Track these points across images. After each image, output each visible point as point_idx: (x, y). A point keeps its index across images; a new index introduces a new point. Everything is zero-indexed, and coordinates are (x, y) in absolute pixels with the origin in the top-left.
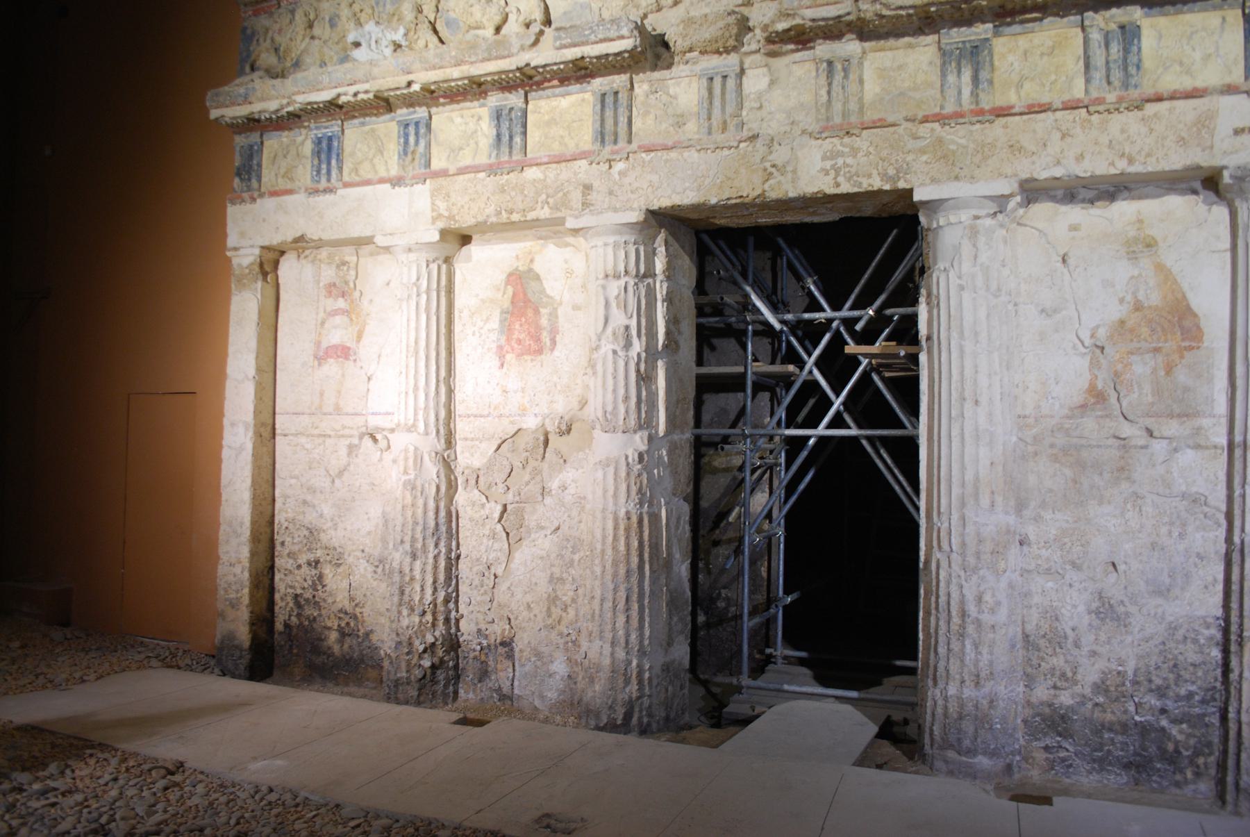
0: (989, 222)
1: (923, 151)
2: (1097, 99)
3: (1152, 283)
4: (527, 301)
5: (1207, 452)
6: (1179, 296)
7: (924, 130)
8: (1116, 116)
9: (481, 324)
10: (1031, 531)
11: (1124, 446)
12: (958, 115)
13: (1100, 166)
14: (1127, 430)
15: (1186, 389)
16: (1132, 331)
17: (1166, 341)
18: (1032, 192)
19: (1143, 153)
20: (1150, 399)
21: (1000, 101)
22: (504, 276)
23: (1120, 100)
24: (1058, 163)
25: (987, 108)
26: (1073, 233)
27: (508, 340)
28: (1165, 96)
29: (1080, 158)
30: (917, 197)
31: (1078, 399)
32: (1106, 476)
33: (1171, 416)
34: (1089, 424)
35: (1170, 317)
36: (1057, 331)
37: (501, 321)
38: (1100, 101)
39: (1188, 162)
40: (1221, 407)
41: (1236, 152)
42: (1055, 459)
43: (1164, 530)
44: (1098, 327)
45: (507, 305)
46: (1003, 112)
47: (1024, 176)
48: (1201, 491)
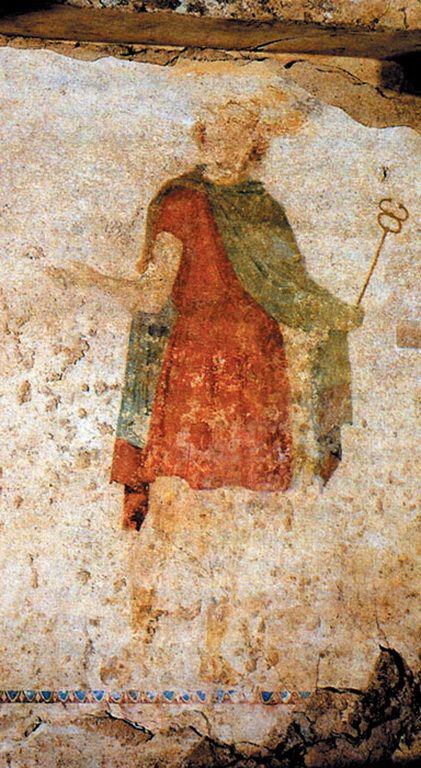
4: (234, 299)
9: (58, 362)
22: (151, 193)
27: (160, 428)
37: (132, 359)
45: (155, 300)
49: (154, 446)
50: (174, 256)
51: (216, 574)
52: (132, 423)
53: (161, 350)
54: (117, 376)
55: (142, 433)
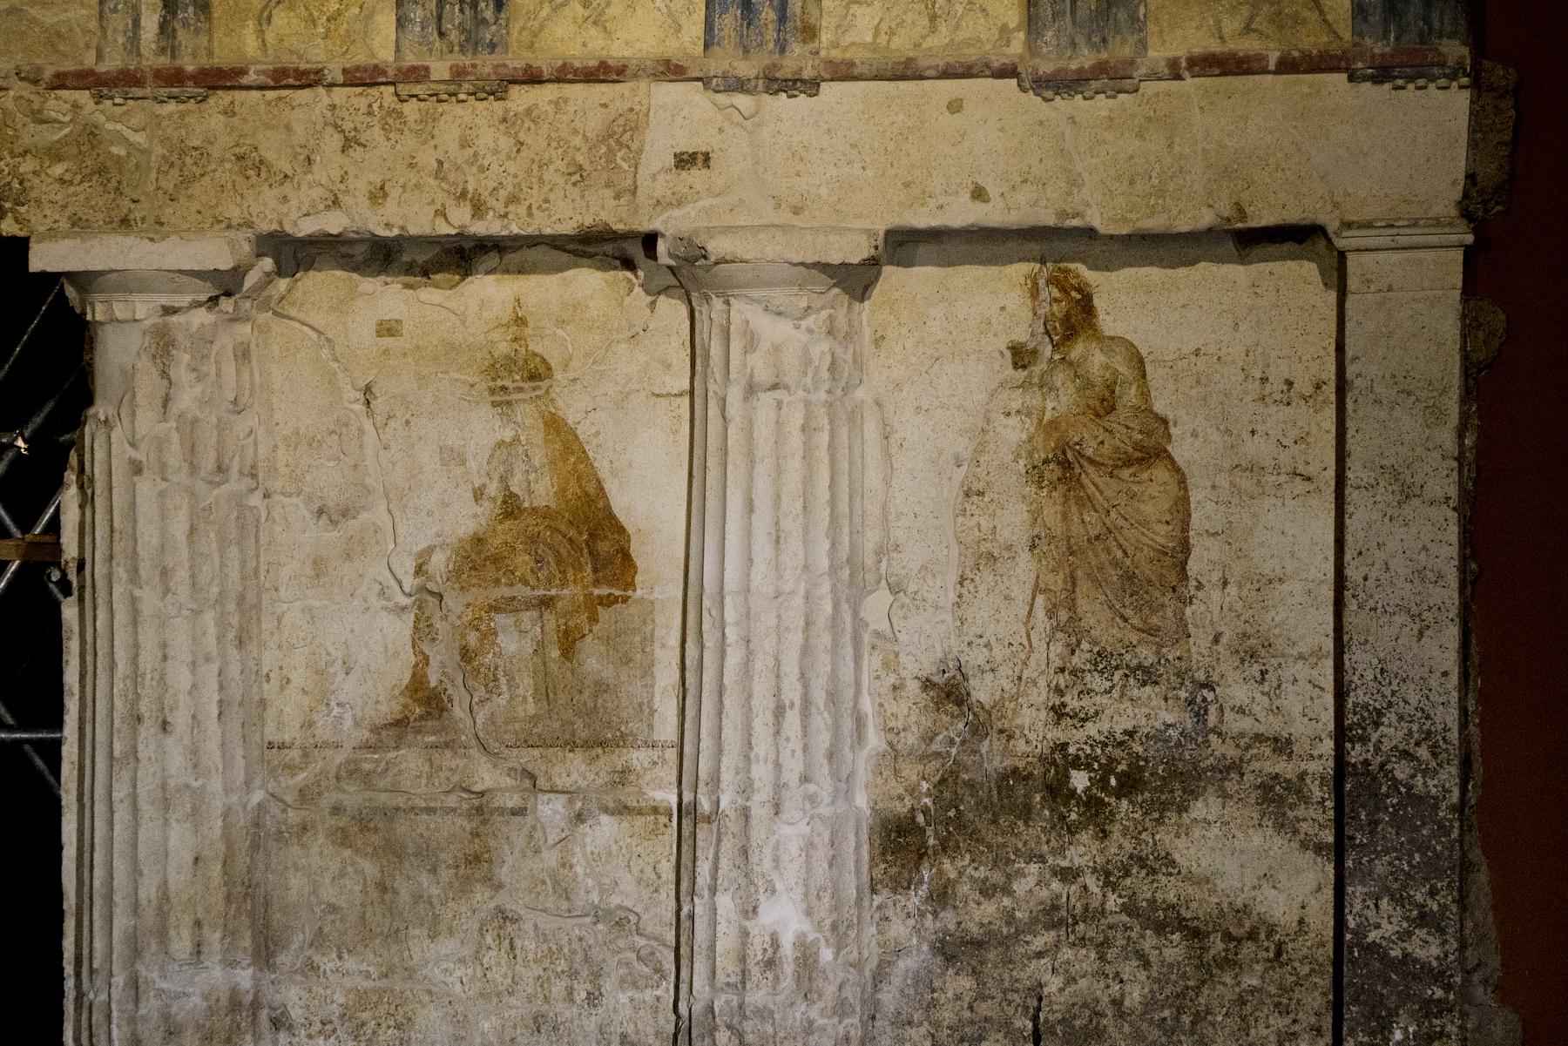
0: (201, 317)
1: (54, 154)
2: (413, 69)
3: (538, 459)
5: (639, 821)
6: (591, 488)
7: (59, 104)
8: (451, 109)
10: (293, 997)
11: (479, 810)
12: (127, 80)
13: (415, 215)
14: (486, 776)
15: (602, 687)
16: (497, 560)
17: (564, 583)
18: (294, 254)
19: (503, 194)
20: (531, 708)
21: (223, 57)
23: (459, 74)
24: (336, 202)
25: (190, 68)
26: (387, 341)
28: (546, 76)
29: (378, 195)
30: (42, 259)
31: (389, 709)
32: (445, 874)
33: (572, 745)
34: (410, 761)
35: (572, 533)
36: (348, 556)
38: (417, 74)
39: (588, 221)
40: (666, 729)
41: (680, 204)
42: (343, 839)
43: (558, 988)
44: (430, 550)
46: (219, 79)
47: (265, 227)
48: (628, 903)
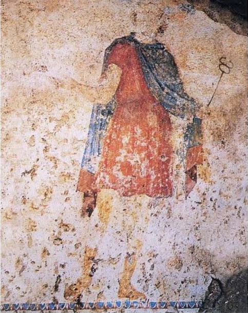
27: (107, 164)
37: (93, 127)
45: (106, 98)
49: (101, 173)
50: (117, 77)
51: (130, 240)
52: (89, 160)
53: (107, 123)
54: (83, 135)
55: (95, 165)
